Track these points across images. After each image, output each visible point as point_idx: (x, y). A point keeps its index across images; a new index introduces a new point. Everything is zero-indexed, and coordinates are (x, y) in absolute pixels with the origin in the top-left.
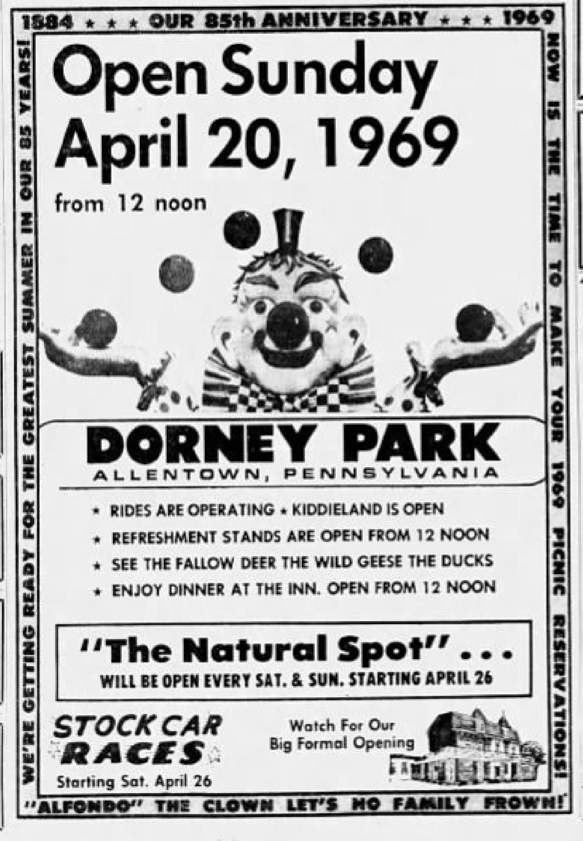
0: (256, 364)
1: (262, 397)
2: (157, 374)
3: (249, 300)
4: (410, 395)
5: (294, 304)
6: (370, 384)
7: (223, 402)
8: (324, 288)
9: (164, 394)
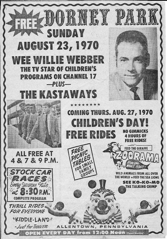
1: (97, 221)
2: (73, 215)
4: (130, 220)
7: (88, 222)
8: (111, 197)
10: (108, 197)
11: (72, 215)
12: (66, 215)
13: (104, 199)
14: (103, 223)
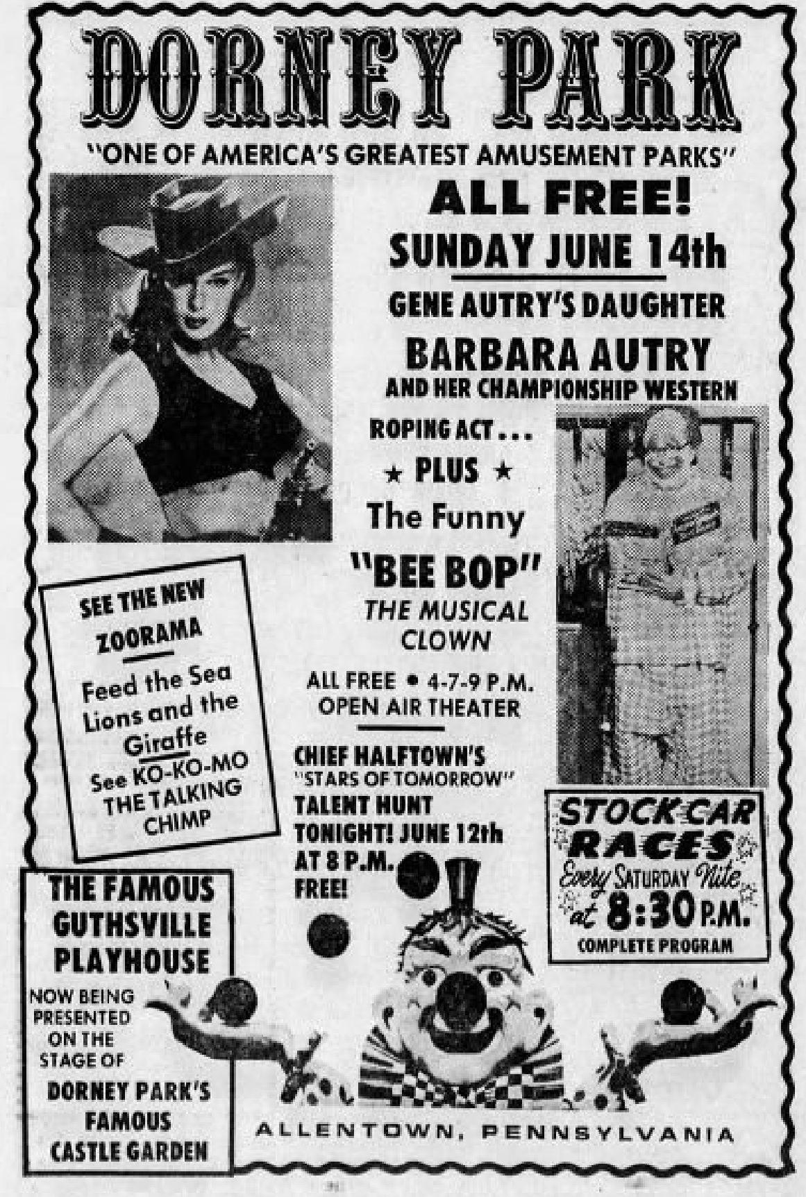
0: (423, 1046)
1: (431, 1088)
2: (305, 1056)
3: (418, 969)
4: (604, 1088)
5: (469, 975)
6: (558, 1074)
8: (505, 955)
9: (312, 1081)
10: (487, 957)
11: (300, 1053)
12: (272, 1051)
13: (468, 967)
14: (464, 1101)
